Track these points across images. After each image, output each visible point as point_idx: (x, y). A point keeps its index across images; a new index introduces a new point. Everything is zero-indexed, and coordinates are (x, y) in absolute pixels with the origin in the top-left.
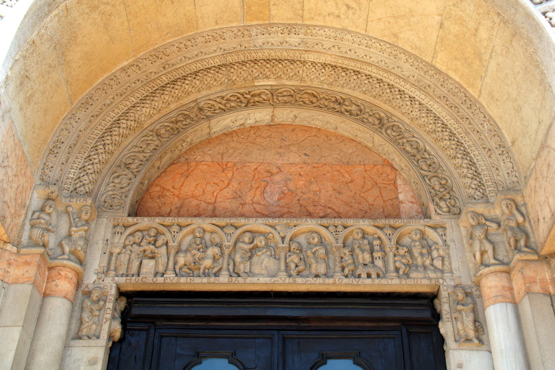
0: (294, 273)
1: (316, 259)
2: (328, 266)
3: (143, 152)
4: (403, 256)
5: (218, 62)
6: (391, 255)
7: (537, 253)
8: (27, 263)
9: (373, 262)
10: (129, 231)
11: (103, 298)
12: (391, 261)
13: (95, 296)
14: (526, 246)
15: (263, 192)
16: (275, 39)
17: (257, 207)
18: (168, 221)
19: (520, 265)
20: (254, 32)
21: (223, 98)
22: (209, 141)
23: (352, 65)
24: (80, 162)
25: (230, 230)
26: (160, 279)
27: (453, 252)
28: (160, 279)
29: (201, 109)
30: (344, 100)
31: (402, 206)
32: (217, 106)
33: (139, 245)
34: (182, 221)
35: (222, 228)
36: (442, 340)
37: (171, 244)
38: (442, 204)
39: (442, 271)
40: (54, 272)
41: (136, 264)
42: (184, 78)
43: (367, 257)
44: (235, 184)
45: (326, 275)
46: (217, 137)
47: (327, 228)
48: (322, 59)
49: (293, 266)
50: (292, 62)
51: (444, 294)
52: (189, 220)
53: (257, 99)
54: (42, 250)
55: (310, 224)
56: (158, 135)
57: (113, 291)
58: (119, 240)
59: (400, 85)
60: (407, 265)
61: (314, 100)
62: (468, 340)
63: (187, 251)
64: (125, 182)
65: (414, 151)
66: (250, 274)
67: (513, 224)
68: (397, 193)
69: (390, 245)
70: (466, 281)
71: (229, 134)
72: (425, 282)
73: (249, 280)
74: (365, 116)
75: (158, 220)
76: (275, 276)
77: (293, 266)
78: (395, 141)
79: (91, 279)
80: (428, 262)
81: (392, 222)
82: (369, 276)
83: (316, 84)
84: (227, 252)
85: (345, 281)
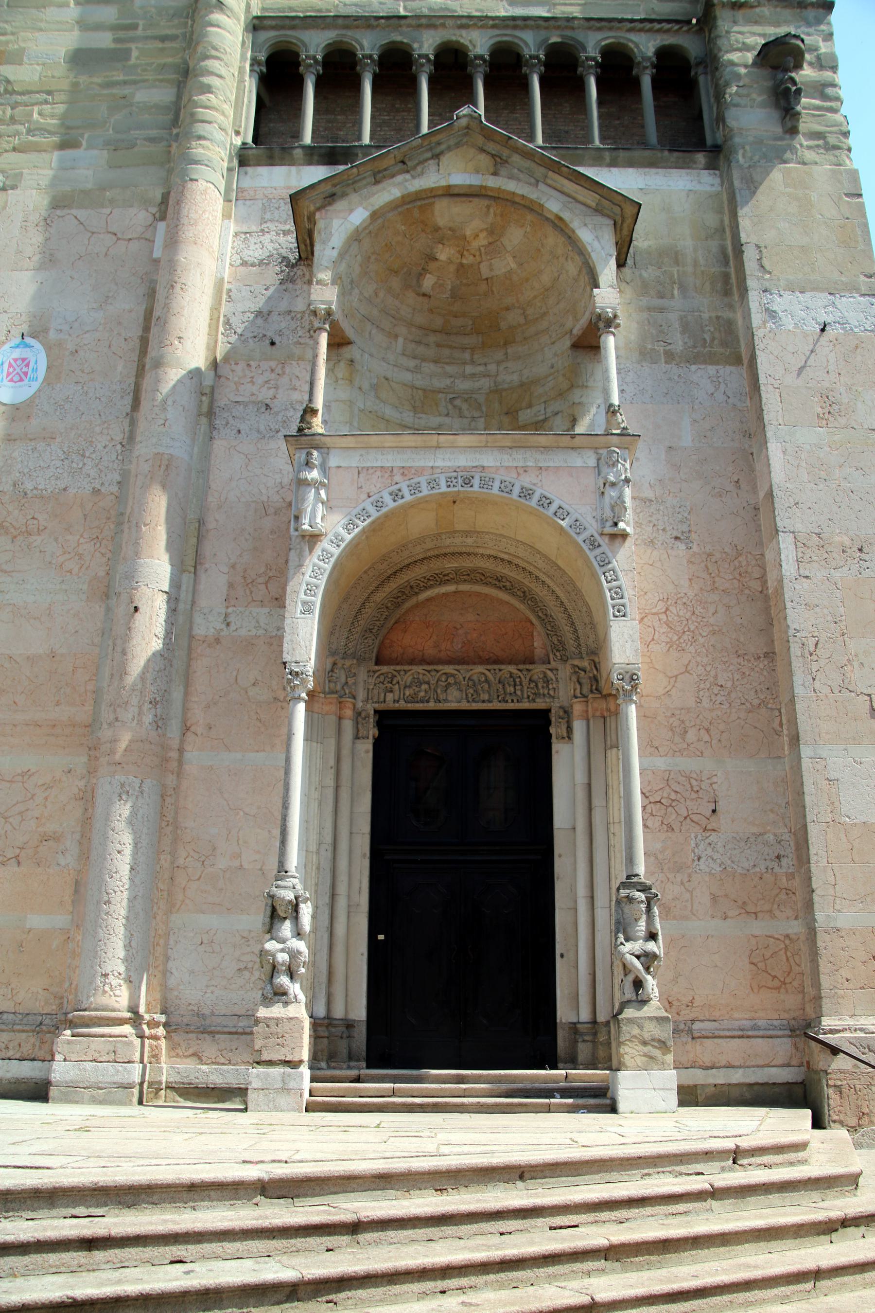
0: (470, 700)
1: (483, 691)
2: (490, 695)
3: (379, 620)
4: (532, 688)
5: (421, 556)
6: (525, 688)
7: (601, 693)
8: (331, 703)
9: (515, 692)
10: (377, 675)
11: (368, 716)
12: (525, 692)
13: (363, 715)
14: (596, 689)
15: (452, 642)
16: (458, 540)
17: (449, 653)
18: (398, 668)
19: (591, 701)
20: (444, 537)
21: (425, 578)
22: (417, 606)
23: (506, 557)
24: (346, 634)
25: (433, 673)
26: (397, 705)
27: (561, 685)
28: (397, 705)
29: (411, 587)
30: (502, 577)
31: (536, 650)
32: (422, 584)
33: (383, 683)
34: (406, 668)
35: (429, 671)
36: (550, 736)
37: (401, 683)
38: (558, 654)
39: (553, 697)
40: (343, 705)
41: (383, 695)
42: (401, 569)
43: (512, 689)
44: (434, 637)
45: (490, 701)
46: (422, 602)
47: (489, 670)
48: (488, 552)
49: (470, 695)
50: (469, 554)
51: (553, 711)
52: (410, 667)
53: (446, 578)
54: (336, 696)
55: (480, 669)
56: (387, 608)
57: (372, 712)
58: (372, 680)
59: (536, 572)
60: (535, 694)
61: (483, 578)
62: (563, 738)
63: (410, 687)
64: (371, 642)
65: (544, 617)
66: (446, 701)
67: (591, 675)
68: (533, 642)
69: (525, 682)
70: (565, 704)
71: (428, 600)
72: (543, 704)
73: (446, 704)
74: (516, 590)
75: (392, 667)
76: (459, 702)
77: (470, 695)
78: (533, 611)
79: (360, 705)
80: (546, 692)
81: (528, 667)
82: (513, 701)
83: (484, 566)
84: (432, 687)
85: (499, 704)
